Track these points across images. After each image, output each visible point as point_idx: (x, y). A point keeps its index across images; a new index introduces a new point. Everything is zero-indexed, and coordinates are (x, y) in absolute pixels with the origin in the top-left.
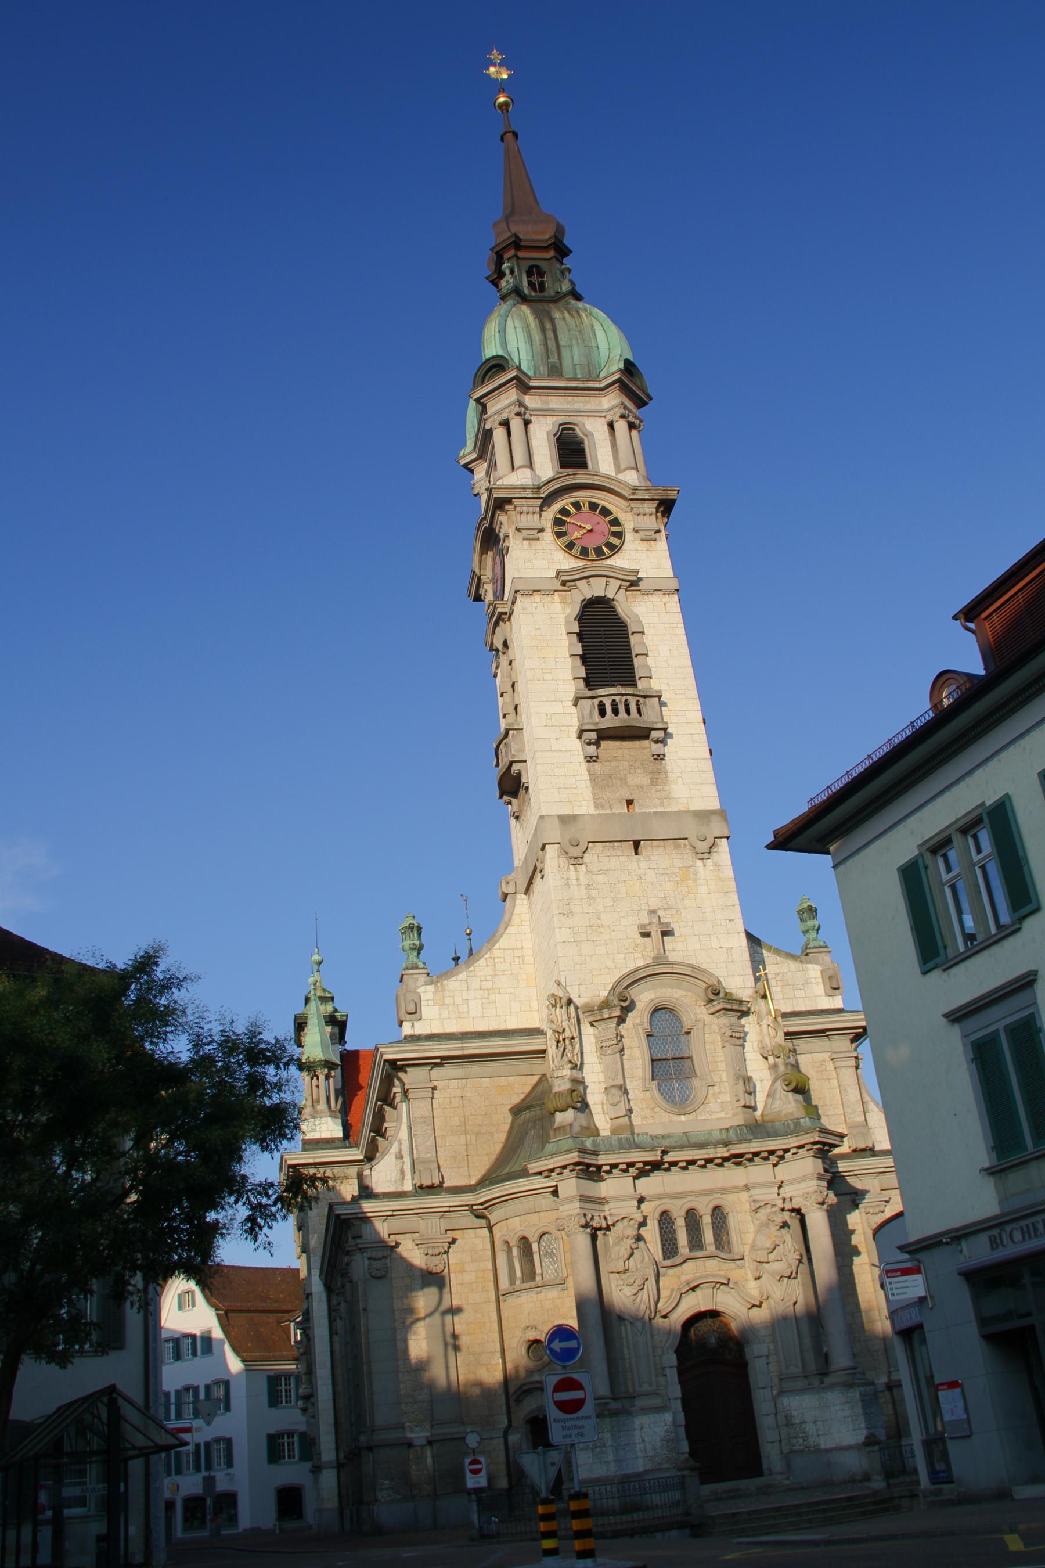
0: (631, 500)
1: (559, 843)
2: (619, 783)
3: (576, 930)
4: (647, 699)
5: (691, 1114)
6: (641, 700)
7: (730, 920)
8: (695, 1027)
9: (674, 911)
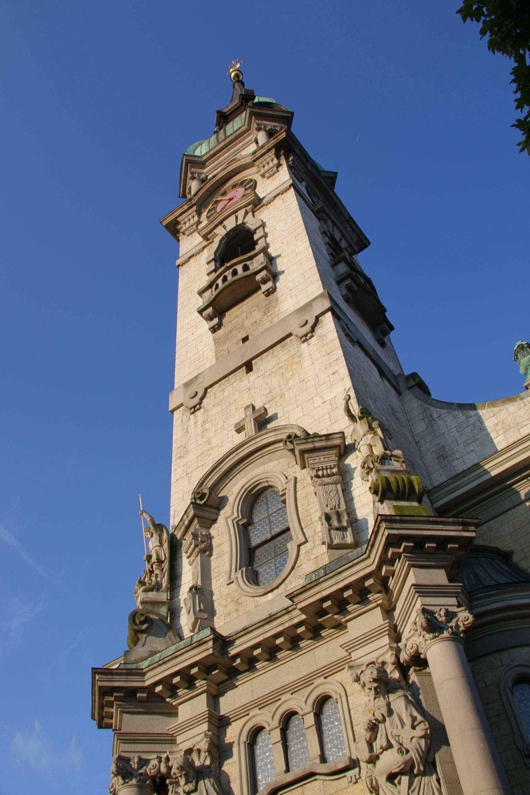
0: (255, 161)
1: (182, 405)
2: (237, 332)
3: (189, 464)
4: (254, 260)
5: (280, 588)
6: (248, 263)
7: (333, 374)
8: (286, 491)
9: (278, 398)
